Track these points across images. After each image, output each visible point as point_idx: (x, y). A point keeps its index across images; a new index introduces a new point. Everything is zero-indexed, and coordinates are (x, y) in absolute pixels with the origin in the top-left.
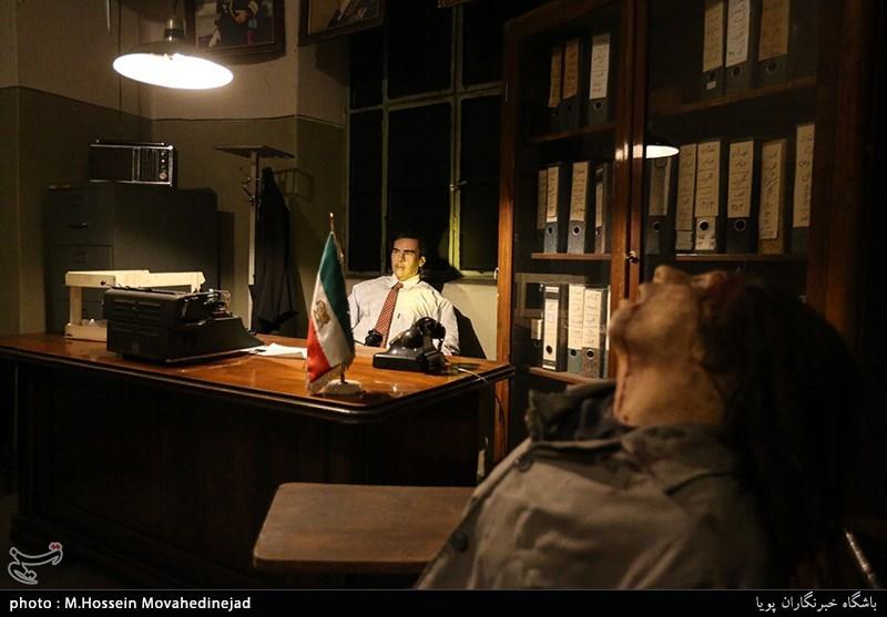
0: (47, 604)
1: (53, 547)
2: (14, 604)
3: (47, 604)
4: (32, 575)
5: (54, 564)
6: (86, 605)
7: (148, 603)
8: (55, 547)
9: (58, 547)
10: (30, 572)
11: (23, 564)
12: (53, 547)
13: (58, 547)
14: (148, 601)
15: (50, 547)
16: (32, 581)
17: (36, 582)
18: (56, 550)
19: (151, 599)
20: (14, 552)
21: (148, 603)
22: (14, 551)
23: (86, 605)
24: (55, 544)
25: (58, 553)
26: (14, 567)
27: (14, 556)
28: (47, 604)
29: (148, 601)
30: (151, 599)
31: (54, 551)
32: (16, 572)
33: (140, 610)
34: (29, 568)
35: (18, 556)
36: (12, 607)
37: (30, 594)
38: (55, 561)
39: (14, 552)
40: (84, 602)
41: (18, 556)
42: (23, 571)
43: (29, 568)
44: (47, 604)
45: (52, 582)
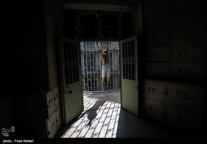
0: (11, 141)
1: (12, 128)
2: (4, 141)
3: (10, 141)
4: (7, 134)
5: (13, 132)
8: (13, 128)
9: (14, 128)
11: (5, 132)
12: (12, 128)
13: (14, 128)
15: (12, 128)
16: (8, 136)
17: (8, 136)
18: (13, 128)
20: (3, 129)
22: (3, 129)
24: (13, 127)
25: (13, 129)
26: (3, 132)
27: (3, 130)
28: (11, 141)
32: (4, 133)
34: (7, 133)
35: (4, 130)
36: (4, 142)
37: (7, 138)
38: (13, 131)
39: (3, 129)
41: (4, 130)
42: (5, 133)
43: (7, 133)
44: (10, 141)
45: (12, 136)
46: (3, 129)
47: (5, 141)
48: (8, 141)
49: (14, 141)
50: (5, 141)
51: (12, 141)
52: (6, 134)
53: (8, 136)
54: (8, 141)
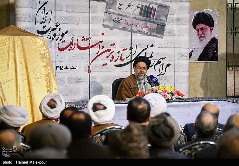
0: (11, 163)
1: (14, 147)
4: (8, 155)
5: (14, 152)
6: (17, 163)
7: (31, 162)
10: (8, 154)
11: (6, 152)
13: (15, 147)
14: (31, 161)
15: (13, 147)
16: (8, 156)
17: (10, 157)
18: (15, 148)
19: (32, 161)
20: (3, 148)
21: (31, 162)
23: (17, 163)
25: (15, 149)
26: (3, 153)
27: (4, 150)
28: (11, 163)
29: (31, 161)
30: (32, 161)
31: (14, 148)
32: (4, 154)
33: (29, 164)
35: (5, 150)
36: (3, 163)
37: (7, 159)
39: (3, 148)
40: (16, 162)
41: (5, 150)
42: (6, 154)
46: (3, 148)
47: (4, 163)
48: (8, 163)
49: (15, 162)
50: (4, 163)
51: (13, 163)
52: (7, 155)
53: (10, 157)
54: (8, 163)
